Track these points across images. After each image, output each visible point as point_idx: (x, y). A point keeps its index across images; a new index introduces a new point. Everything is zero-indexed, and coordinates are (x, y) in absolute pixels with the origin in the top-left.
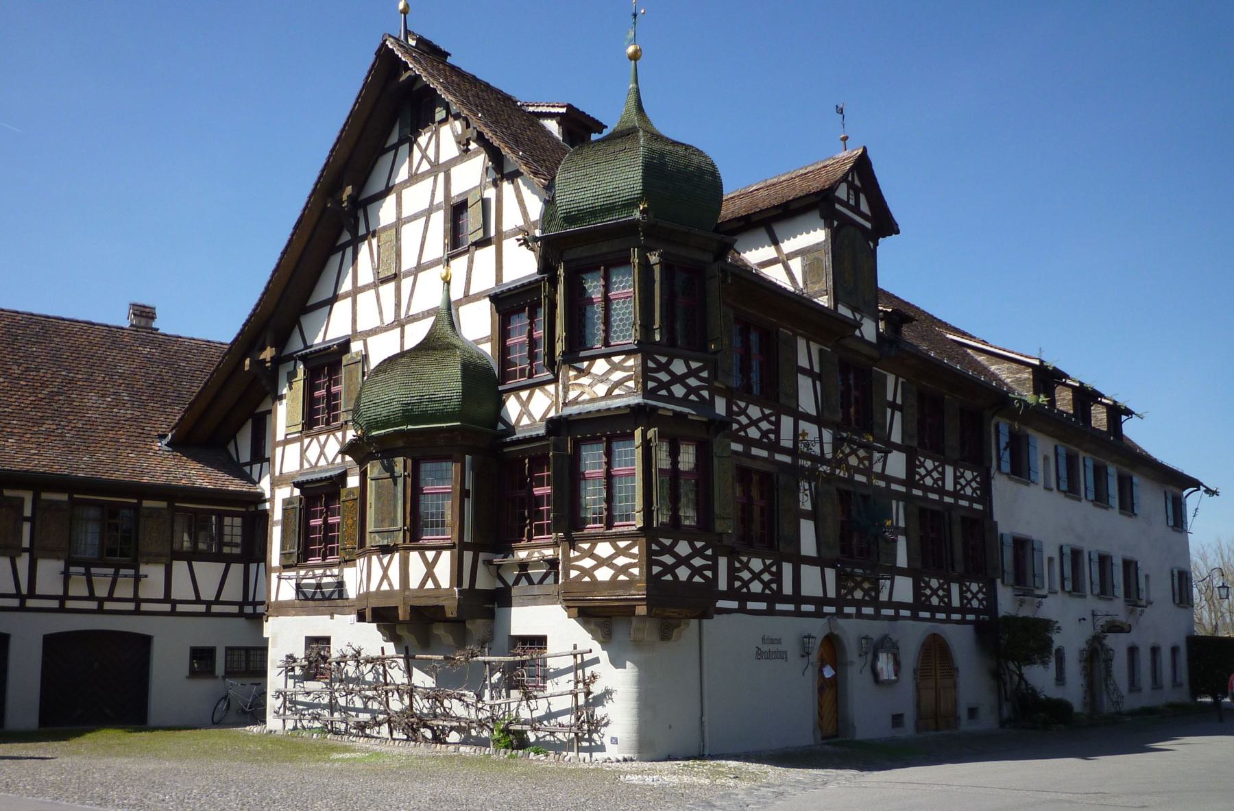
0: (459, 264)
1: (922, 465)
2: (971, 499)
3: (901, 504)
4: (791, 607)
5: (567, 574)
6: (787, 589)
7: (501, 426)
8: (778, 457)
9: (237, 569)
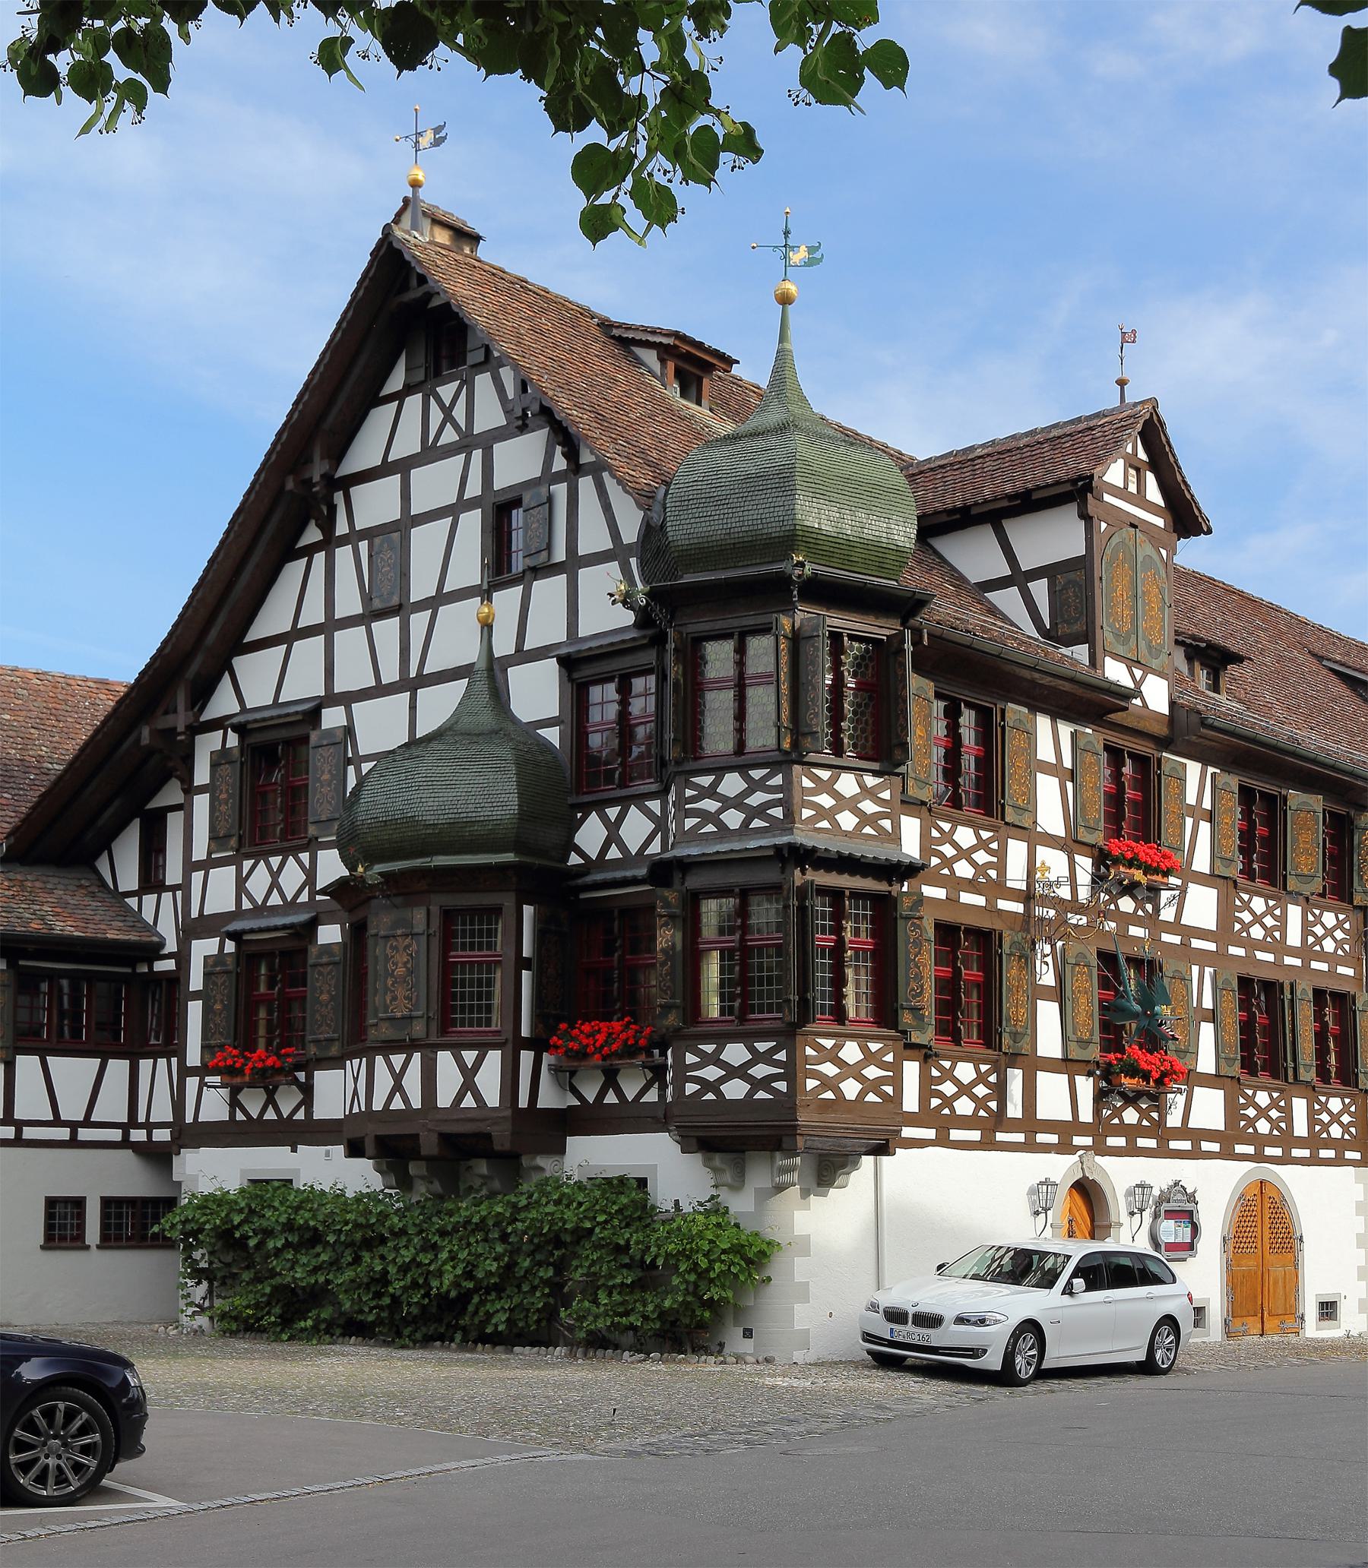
0: (507, 600)
1: (1247, 906)
2: (1331, 959)
3: (1208, 971)
4: (1020, 1137)
5: (680, 1090)
6: (1014, 1109)
7: (574, 859)
8: (1003, 905)
9: (118, 1068)
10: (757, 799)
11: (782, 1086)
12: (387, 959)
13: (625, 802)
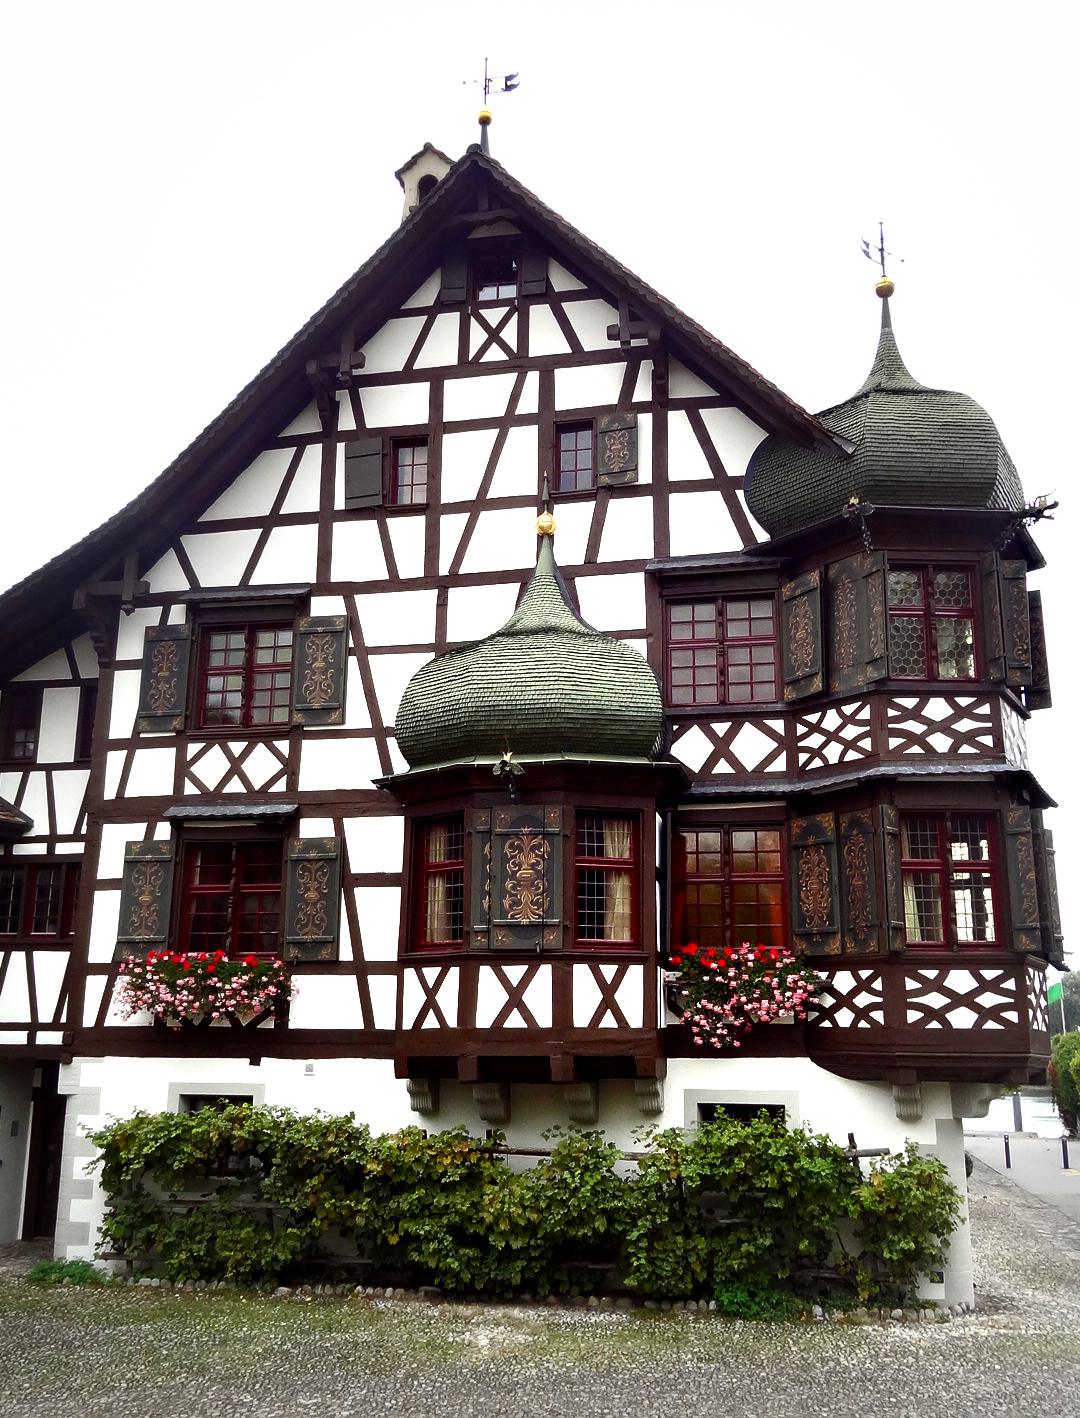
10: (965, 725)
11: (1012, 1016)
12: (505, 859)
13: (737, 719)
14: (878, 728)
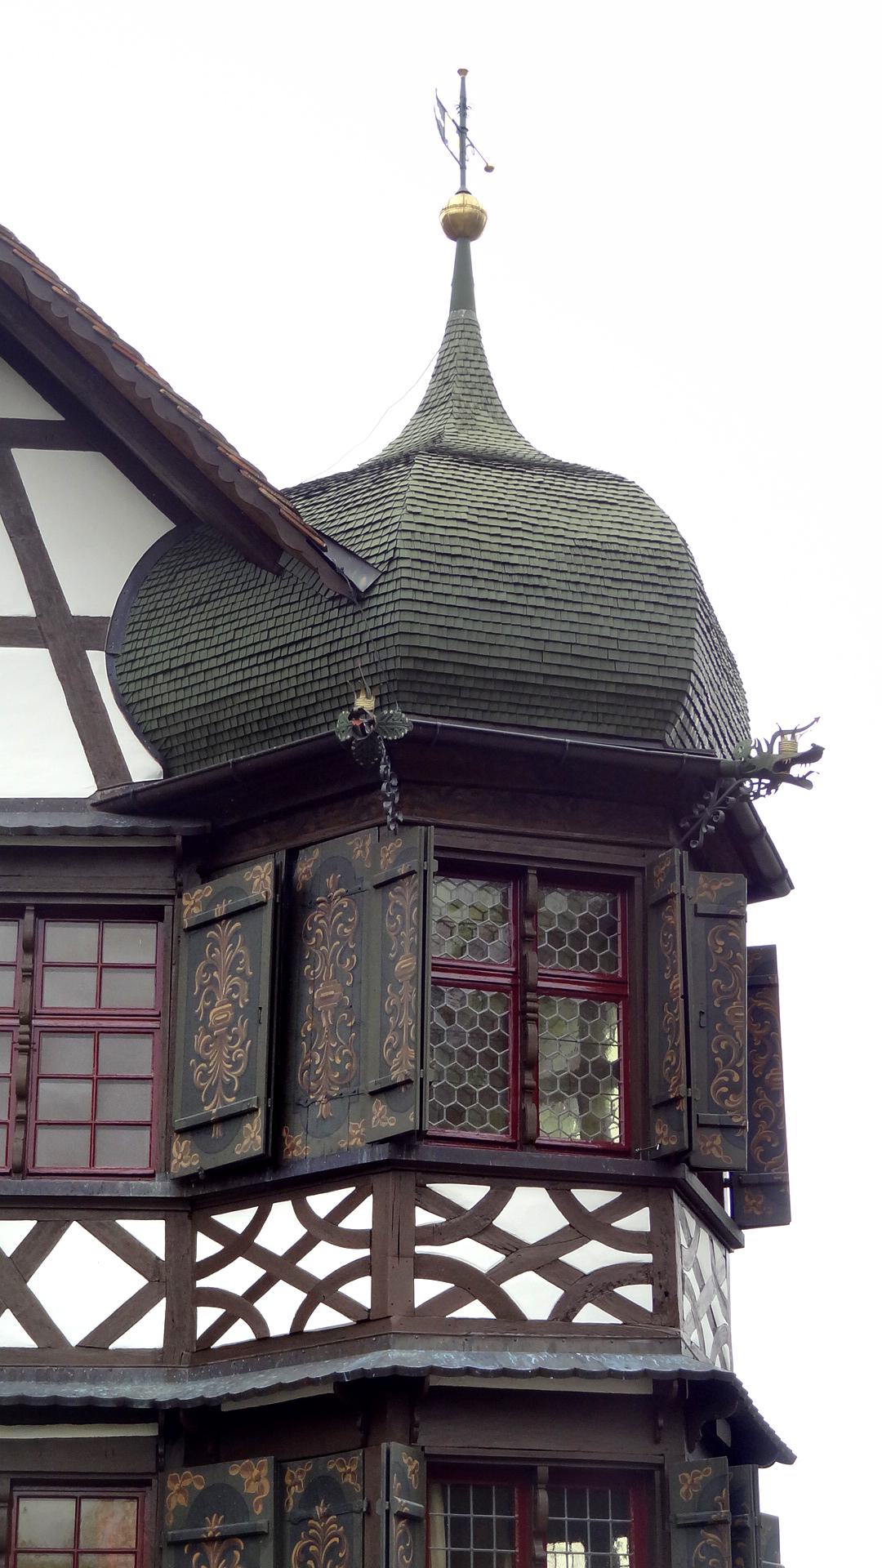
10: (591, 1257)
14: (391, 1254)
